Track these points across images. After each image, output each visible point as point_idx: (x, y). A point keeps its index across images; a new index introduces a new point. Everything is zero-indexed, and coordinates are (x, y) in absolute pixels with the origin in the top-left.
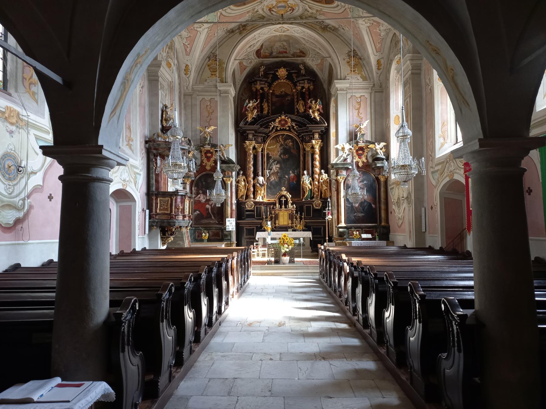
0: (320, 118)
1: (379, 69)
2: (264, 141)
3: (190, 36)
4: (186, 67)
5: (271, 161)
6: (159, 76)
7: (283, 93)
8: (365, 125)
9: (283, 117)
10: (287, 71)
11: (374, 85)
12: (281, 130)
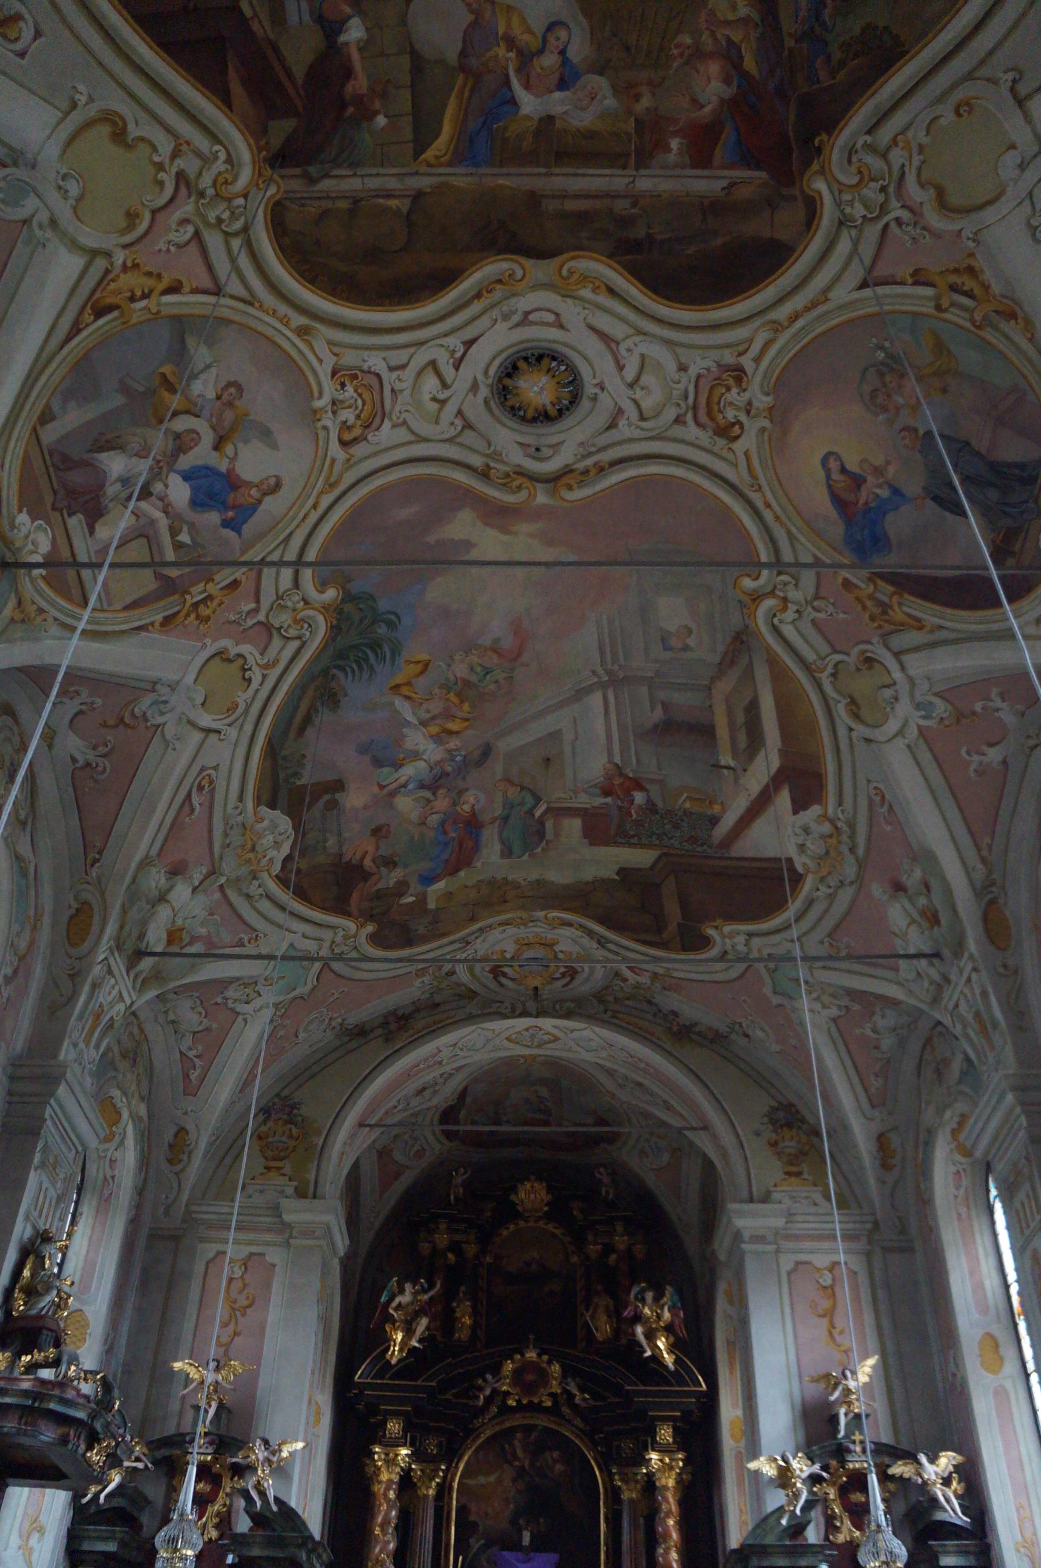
0: (677, 1361)
1: (885, 1165)
2: (450, 1455)
3: (208, 1029)
4: (176, 1135)
5: (475, 1544)
6: (47, 1116)
7: (534, 1266)
8: (863, 1378)
9: (531, 1355)
10: (550, 1189)
11: (876, 1224)
12: (520, 1407)
